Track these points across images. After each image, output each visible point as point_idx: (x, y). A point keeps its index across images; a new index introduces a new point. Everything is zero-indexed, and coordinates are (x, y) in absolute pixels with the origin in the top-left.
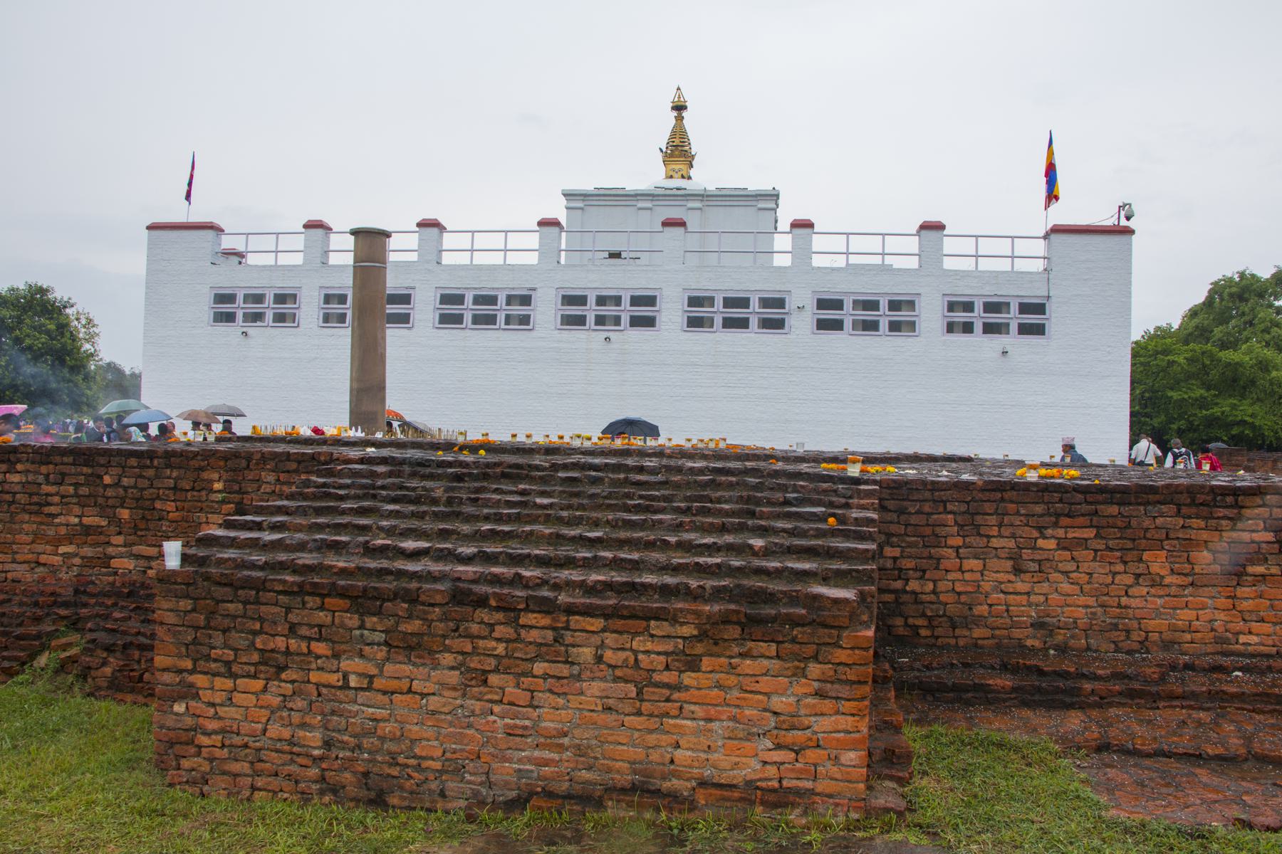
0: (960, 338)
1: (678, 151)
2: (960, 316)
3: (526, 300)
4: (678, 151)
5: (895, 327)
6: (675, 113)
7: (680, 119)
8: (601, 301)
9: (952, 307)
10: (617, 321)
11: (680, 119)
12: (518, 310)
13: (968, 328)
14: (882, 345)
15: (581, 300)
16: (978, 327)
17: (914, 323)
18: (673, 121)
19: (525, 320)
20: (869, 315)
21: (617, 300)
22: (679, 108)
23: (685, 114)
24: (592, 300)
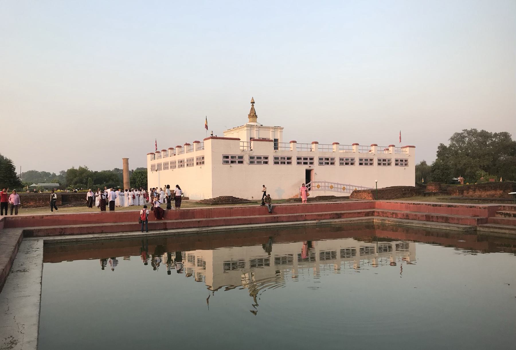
1: (253, 115)
2: (342, 162)
3: (266, 158)
4: (253, 115)
5: (331, 164)
7: (253, 105)
9: (340, 159)
11: (253, 105)
12: (266, 160)
13: (343, 164)
14: (329, 166)
16: (344, 164)
19: (266, 163)
20: (327, 161)
21: (284, 158)
22: (253, 103)
24: (280, 158)
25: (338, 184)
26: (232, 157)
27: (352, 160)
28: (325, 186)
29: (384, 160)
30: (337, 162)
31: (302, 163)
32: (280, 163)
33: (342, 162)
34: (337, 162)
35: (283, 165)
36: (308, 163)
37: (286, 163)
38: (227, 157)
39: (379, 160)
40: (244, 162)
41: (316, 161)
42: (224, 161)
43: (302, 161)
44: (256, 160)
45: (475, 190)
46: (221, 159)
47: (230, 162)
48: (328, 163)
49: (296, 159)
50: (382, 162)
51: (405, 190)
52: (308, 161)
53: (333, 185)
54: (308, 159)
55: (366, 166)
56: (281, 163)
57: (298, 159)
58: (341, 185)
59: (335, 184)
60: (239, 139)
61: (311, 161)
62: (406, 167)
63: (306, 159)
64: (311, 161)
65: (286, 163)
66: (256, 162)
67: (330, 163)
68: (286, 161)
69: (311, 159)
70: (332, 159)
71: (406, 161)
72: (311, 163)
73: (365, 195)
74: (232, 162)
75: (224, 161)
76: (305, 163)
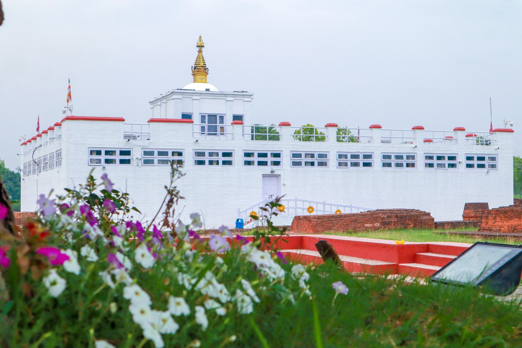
0: (343, 169)
1: (200, 70)
2: (343, 160)
4: (200, 70)
5: (321, 164)
6: (198, 49)
7: (200, 51)
8: (211, 154)
9: (340, 156)
10: (218, 163)
11: (200, 51)
13: (346, 164)
15: (202, 154)
16: (349, 164)
17: (326, 163)
18: (197, 53)
20: (310, 160)
21: (217, 154)
23: (203, 49)
24: (207, 154)
25: (324, 204)
26: (107, 153)
27: (366, 157)
28: (296, 208)
29: (439, 158)
30: (333, 160)
31: (256, 163)
32: (207, 162)
33: (343, 160)
34: (333, 160)
35: (214, 167)
36: (269, 163)
37: (220, 163)
38: (99, 153)
39: (431, 158)
40: (134, 162)
41: (286, 159)
42: (91, 160)
43: (256, 159)
44: (156, 158)
45: (495, 218)
46: (87, 157)
47: (103, 161)
48: (312, 164)
49: (242, 155)
50: (435, 162)
51: (388, 217)
52: (269, 159)
53: (314, 206)
54: (269, 155)
55: (399, 169)
56: (211, 163)
57: (247, 155)
58: (331, 205)
59: (317, 203)
60: (123, 120)
61: (276, 159)
62: (492, 171)
63: (265, 155)
64: (276, 159)
65: (220, 163)
66: (156, 161)
67: (316, 164)
68: (221, 159)
69: (277, 155)
70: (320, 156)
71: (493, 159)
72: (277, 163)
73: (306, 223)
74: (107, 161)
75: (91, 160)
76: (260, 163)
